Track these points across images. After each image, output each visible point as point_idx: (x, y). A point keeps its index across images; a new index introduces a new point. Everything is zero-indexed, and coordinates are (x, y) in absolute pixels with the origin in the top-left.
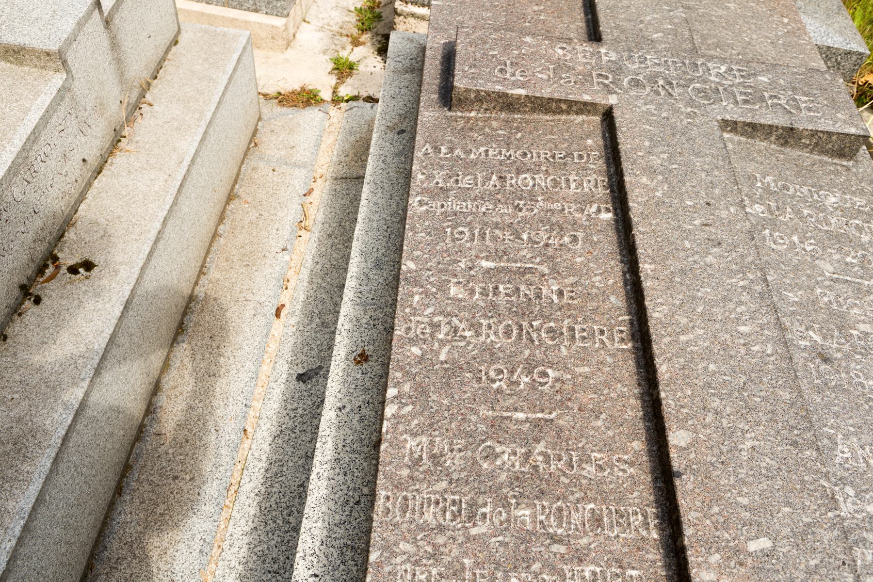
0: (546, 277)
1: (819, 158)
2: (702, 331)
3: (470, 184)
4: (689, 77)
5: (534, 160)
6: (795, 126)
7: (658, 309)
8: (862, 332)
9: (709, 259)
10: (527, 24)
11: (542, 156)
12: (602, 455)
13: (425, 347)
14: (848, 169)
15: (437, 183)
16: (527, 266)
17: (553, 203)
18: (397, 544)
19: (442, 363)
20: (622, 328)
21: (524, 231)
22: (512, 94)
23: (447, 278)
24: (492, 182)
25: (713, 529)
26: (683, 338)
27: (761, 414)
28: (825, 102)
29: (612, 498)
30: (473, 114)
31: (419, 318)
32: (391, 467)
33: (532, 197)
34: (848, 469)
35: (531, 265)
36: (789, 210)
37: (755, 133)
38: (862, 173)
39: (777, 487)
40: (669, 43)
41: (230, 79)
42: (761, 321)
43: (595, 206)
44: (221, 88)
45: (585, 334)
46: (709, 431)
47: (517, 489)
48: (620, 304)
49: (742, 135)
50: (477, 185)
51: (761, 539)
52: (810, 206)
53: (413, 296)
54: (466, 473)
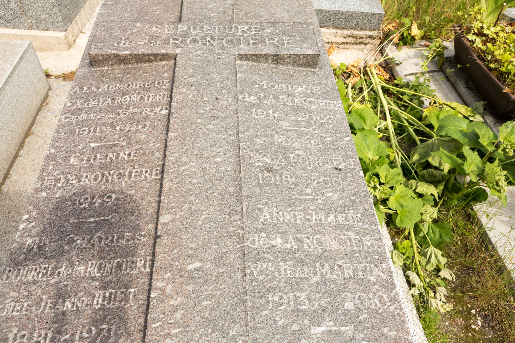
0: (124, 148)
1: (298, 68)
2: (194, 163)
3: (95, 105)
4: (225, 34)
5: (133, 88)
6: (278, 53)
7: (172, 155)
8: (296, 155)
9: (210, 126)
10: (149, 17)
11: (138, 85)
12: (131, 234)
13: (49, 191)
14: (315, 72)
15: (77, 106)
16: (115, 143)
17: (138, 109)
18: (9, 293)
19: (56, 198)
20: (158, 168)
21: (118, 126)
22: (122, 55)
23: (69, 155)
24: (107, 102)
25: (171, 261)
26: (182, 168)
27: (215, 201)
28: (299, 39)
29: (130, 254)
30: (106, 68)
31: (50, 178)
32: (15, 255)
33: (127, 107)
34: (266, 224)
35: (117, 142)
36: (271, 97)
37: (259, 60)
38: (323, 74)
39: (213, 236)
40: (219, 18)
41: (15, 68)
42: (229, 155)
43: (160, 107)
44: (8, 73)
45: (137, 174)
46: (183, 213)
47: (80, 257)
48: (160, 156)
49: (253, 61)
50: (98, 105)
51: (196, 263)
52: (285, 94)
53: (49, 166)
54: (55, 253)
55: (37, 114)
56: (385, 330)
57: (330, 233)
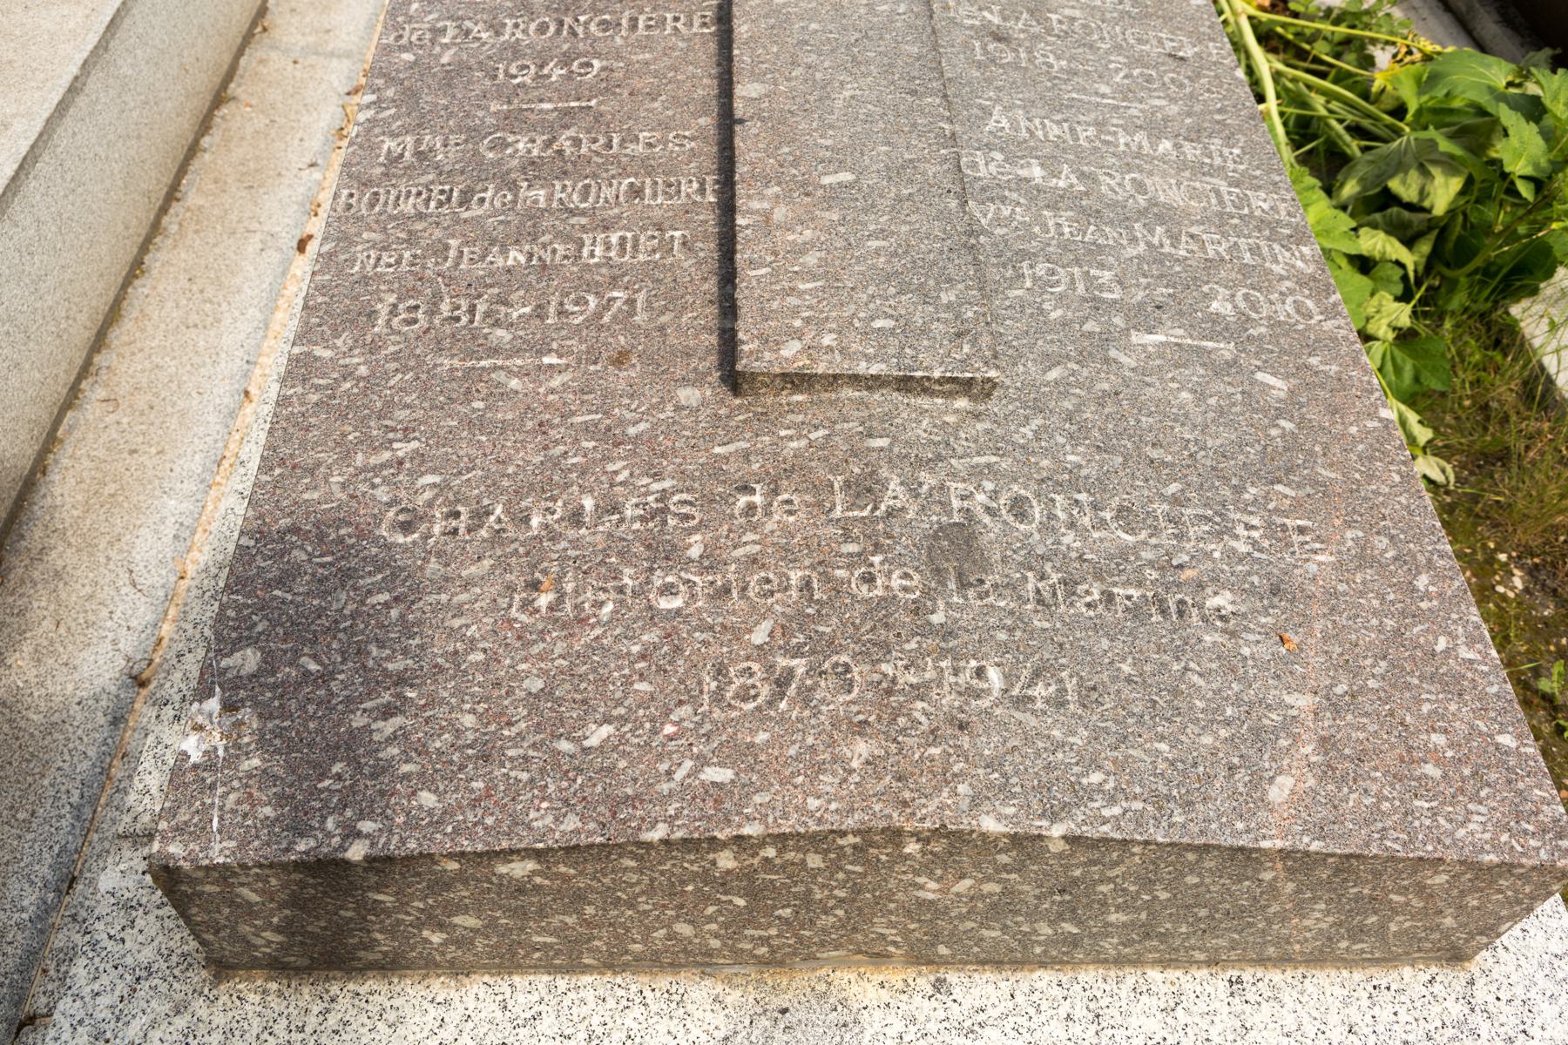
55: (240, 52)
56: (1314, 361)
57: (1164, 175)
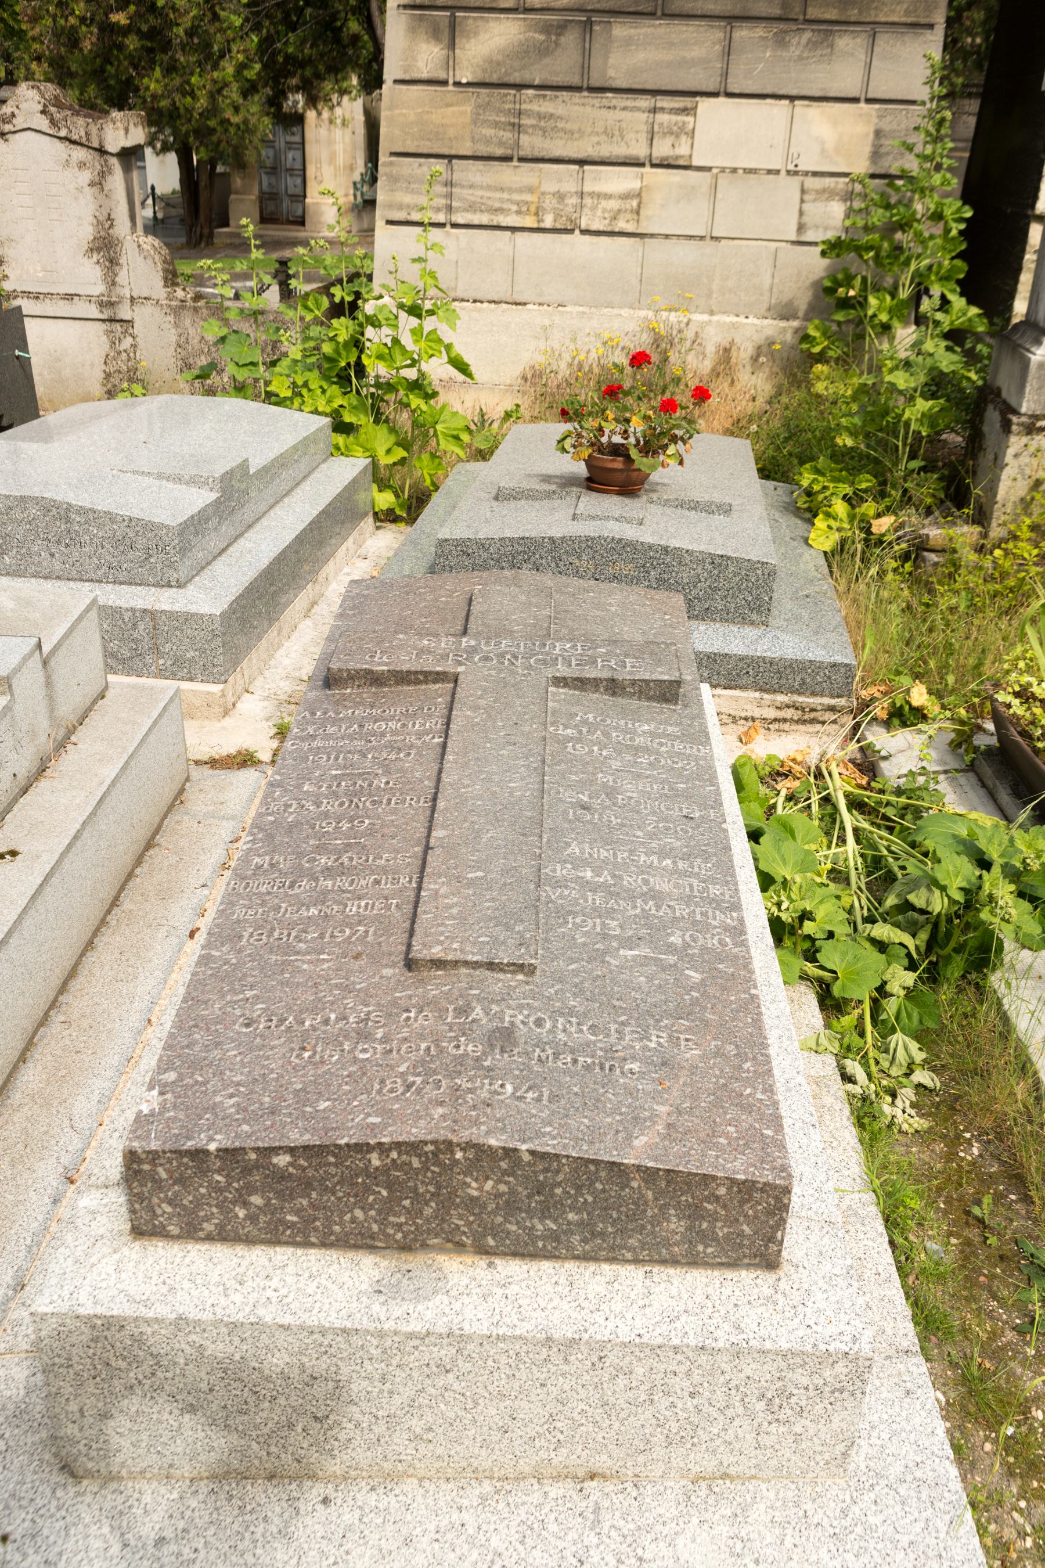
30: (349, 691)
41: (155, 723)
44: (145, 729)
55: (165, 816)
56: (721, 966)
57: (662, 876)
